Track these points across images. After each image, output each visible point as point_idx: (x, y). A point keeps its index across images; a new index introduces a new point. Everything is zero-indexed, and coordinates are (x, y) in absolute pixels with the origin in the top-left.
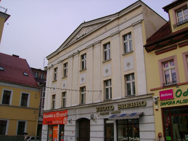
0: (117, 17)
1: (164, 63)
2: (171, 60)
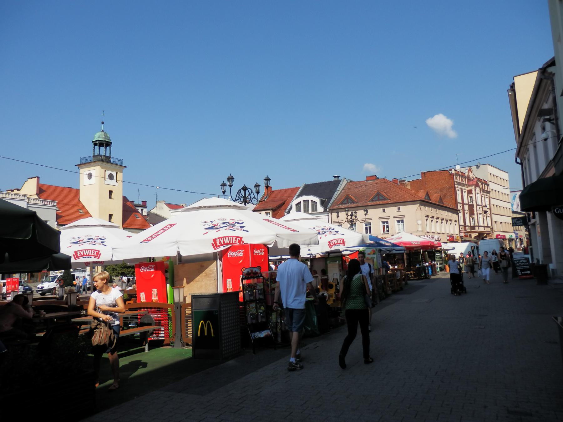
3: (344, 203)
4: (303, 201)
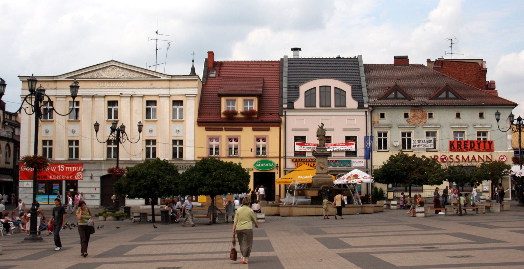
0: (170, 79)
1: (211, 139)
2: (217, 139)
3: (390, 96)
4: (320, 87)
